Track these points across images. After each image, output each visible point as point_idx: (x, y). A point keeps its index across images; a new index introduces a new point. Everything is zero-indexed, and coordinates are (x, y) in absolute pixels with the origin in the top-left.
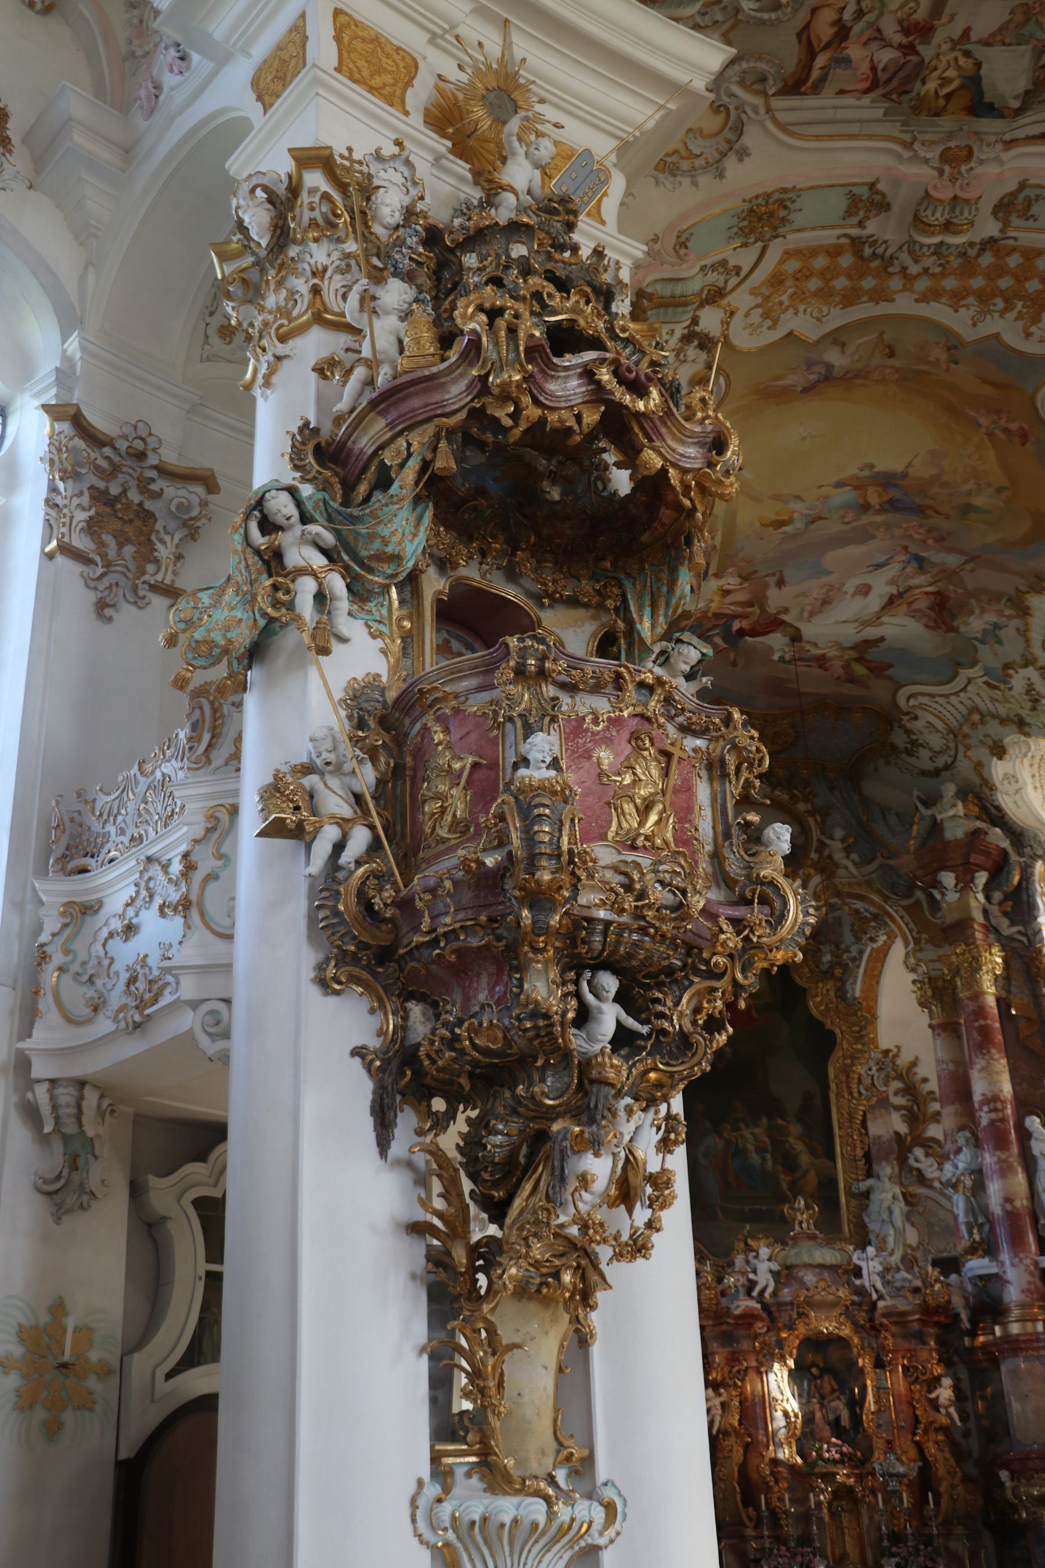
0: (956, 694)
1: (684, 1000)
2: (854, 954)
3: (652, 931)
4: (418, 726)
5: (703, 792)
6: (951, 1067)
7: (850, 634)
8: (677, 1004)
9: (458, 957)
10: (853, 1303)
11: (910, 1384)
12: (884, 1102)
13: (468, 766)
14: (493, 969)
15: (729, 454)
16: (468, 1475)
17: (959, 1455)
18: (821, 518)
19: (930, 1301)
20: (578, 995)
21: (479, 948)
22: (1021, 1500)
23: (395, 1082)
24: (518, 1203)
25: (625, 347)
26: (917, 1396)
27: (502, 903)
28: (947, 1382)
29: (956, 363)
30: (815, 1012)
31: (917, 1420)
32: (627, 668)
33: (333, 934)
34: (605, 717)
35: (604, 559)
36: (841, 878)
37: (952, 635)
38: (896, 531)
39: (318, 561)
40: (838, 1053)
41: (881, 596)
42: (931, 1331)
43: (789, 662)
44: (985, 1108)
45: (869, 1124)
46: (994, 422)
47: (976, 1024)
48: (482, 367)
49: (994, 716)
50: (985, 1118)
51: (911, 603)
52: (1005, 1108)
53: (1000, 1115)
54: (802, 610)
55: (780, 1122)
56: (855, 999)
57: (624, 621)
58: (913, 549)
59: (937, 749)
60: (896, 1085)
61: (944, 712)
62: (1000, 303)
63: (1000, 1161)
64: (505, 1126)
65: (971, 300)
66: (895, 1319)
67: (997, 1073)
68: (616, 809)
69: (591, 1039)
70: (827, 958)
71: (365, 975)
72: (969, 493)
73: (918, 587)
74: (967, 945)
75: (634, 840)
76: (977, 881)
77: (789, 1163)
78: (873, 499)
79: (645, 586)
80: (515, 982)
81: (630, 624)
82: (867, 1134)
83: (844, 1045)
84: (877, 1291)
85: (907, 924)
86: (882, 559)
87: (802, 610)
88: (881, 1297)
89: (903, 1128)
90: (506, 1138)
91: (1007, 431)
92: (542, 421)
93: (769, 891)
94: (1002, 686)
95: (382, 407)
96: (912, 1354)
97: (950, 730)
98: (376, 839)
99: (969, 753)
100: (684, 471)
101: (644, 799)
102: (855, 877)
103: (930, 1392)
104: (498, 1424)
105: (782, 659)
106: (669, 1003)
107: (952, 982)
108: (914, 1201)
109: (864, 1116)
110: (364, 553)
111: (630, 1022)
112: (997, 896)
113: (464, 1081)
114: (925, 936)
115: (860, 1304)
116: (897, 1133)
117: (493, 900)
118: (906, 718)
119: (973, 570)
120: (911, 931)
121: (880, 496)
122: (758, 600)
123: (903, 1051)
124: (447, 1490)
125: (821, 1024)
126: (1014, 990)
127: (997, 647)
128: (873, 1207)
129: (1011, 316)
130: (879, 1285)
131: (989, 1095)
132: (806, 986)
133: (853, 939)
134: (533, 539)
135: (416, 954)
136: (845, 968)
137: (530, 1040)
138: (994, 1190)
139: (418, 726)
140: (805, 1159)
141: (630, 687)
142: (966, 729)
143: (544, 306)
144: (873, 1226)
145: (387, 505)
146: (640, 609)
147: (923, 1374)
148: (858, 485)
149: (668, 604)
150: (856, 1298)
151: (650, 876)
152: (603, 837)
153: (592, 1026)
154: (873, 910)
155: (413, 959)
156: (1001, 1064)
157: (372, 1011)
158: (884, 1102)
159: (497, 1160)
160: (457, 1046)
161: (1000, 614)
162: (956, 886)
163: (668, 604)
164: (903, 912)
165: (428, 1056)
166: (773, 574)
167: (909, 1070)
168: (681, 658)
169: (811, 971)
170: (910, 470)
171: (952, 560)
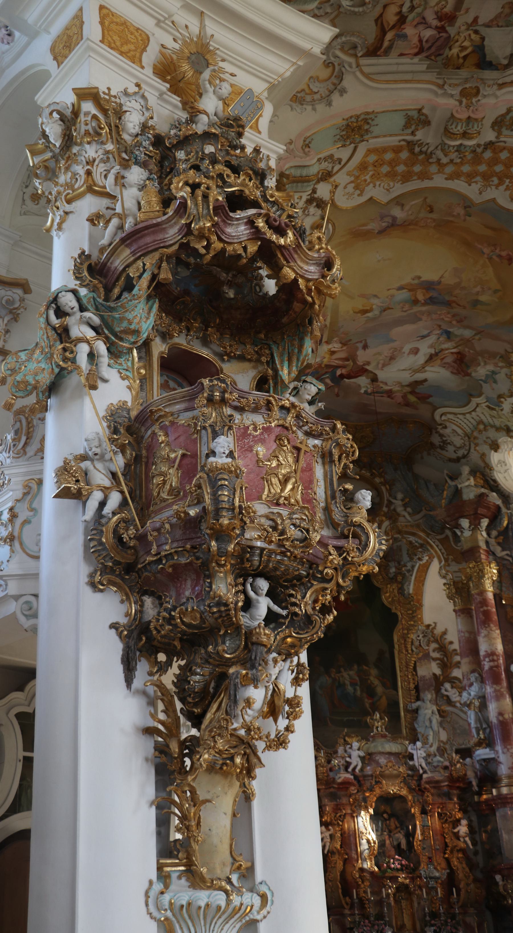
0: (470, 413)
1: (308, 595)
2: (409, 567)
3: (289, 554)
4: (149, 432)
5: (319, 471)
6: (467, 635)
7: (407, 377)
8: (304, 597)
9: (173, 570)
11: (442, 823)
12: (427, 656)
13: (179, 456)
14: (194, 576)
15: (335, 270)
16: (179, 878)
17: (472, 866)
18: (389, 308)
19: (454, 774)
20: (245, 592)
21: (186, 564)
22: (508, 893)
23: (136, 644)
24: (209, 716)
25: (273, 207)
26: (446, 831)
27: (200, 537)
28: (464, 822)
29: (470, 216)
30: (385, 602)
31: (446, 845)
32: (274, 397)
33: (99, 556)
34: (261, 426)
35: (260, 332)
36: (401, 522)
37: (467, 378)
38: (434, 316)
39: (90, 334)
40: (399, 626)
41: (425, 355)
42: (455, 792)
43: (370, 394)
44: (487, 659)
45: (418, 669)
46: (492, 251)
47: (482, 610)
48: (188, 218)
49: (492, 426)
50: (487, 665)
51: (443, 359)
52: (498, 659)
53: (496, 663)
54: (378, 363)
55: (365, 667)
56: (409, 594)
57: (272, 370)
58: (444, 327)
59: (458, 445)
60: (434, 645)
61: (463, 424)
62: (496, 180)
63: (495, 691)
64: (201, 670)
65: (478, 178)
66: (433, 785)
67: (494, 639)
68: (267, 482)
69: (252, 618)
70: (393, 570)
71: (118, 580)
72: (478, 293)
73: (447, 349)
74: (476, 562)
75: (278, 500)
76: (482, 524)
77: (371, 692)
78: (420, 297)
79: (284, 349)
80: (207, 584)
81: (276, 371)
82: (417, 675)
83: (403, 622)
84: (422, 768)
85: (440, 550)
86: (425, 332)
87: (378, 363)
88: (425, 772)
89: (438, 671)
90: (202, 677)
91: (500, 256)
92: (223, 251)
93: (358, 530)
94: (497, 408)
95: (128, 242)
96: (443, 806)
97: (466, 435)
98: (125, 499)
99: (477, 448)
100: (308, 280)
101: (284, 476)
102: (409, 522)
103: (454, 828)
104: (197, 847)
105: (366, 392)
106: (299, 597)
107: (467, 585)
108: (444, 714)
109: (415, 664)
110: (117, 329)
111: (276, 608)
112: (494, 533)
113: (177, 643)
114: (451, 557)
115: (412, 776)
116: (434, 674)
117: (194, 536)
118: (440, 427)
119: (480, 339)
120: (443, 554)
121: (424, 295)
122: (352, 357)
123: (438, 625)
124: (167, 886)
125: (389, 610)
126: (504, 589)
127: (494, 385)
128: (420, 718)
129: (502, 188)
130: (424, 765)
131: (489, 652)
132: (380, 586)
133: (408, 559)
134: (218, 321)
135: (148, 568)
136: (404, 576)
137: (216, 619)
138: (492, 708)
139: (149, 432)
140: (380, 690)
141: (276, 409)
142: (476, 434)
143: (224, 182)
144: (420, 730)
145: (131, 300)
146: (282, 362)
147: (450, 818)
148: (411, 289)
149: (298, 360)
150: (410, 772)
151: (287, 522)
152: (260, 498)
153: (253, 611)
154: (420, 541)
155: (146, 571)
156: (497, 633)
157: (122, 602)
158: (427, 656)
159: (196, 690)
160: (173, 622)
161: (496, 365)
162: (469, 527)
163: (298, 360)
164: (438, 543)
165: (156, 628)
166: (361, 342)
167: (441, 637)
168: (306, 392)
169: (383, 578)
170: (442, 280)
171: (467, 333)
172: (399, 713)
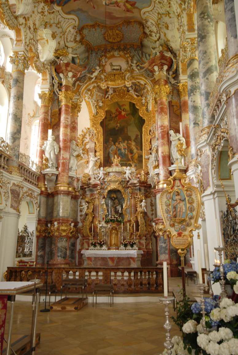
10: (122, 181)
43: (108, 5)
55: (130, 142)
70: (144, 101)
77: (131, 152)
84: (129, 178)
85: (151, 85)
88: (131, 180)
115: (125, 181)
120: (152, 86)
125: (142, 118)
126: (173, 98)
140: (135, 151)
154: (145, 82)
164: (150, 81)
172: (142, 160)
